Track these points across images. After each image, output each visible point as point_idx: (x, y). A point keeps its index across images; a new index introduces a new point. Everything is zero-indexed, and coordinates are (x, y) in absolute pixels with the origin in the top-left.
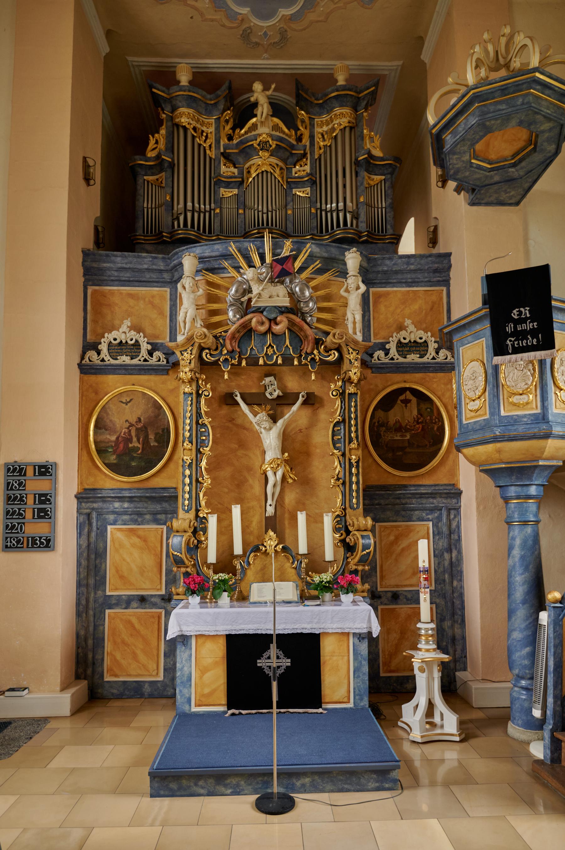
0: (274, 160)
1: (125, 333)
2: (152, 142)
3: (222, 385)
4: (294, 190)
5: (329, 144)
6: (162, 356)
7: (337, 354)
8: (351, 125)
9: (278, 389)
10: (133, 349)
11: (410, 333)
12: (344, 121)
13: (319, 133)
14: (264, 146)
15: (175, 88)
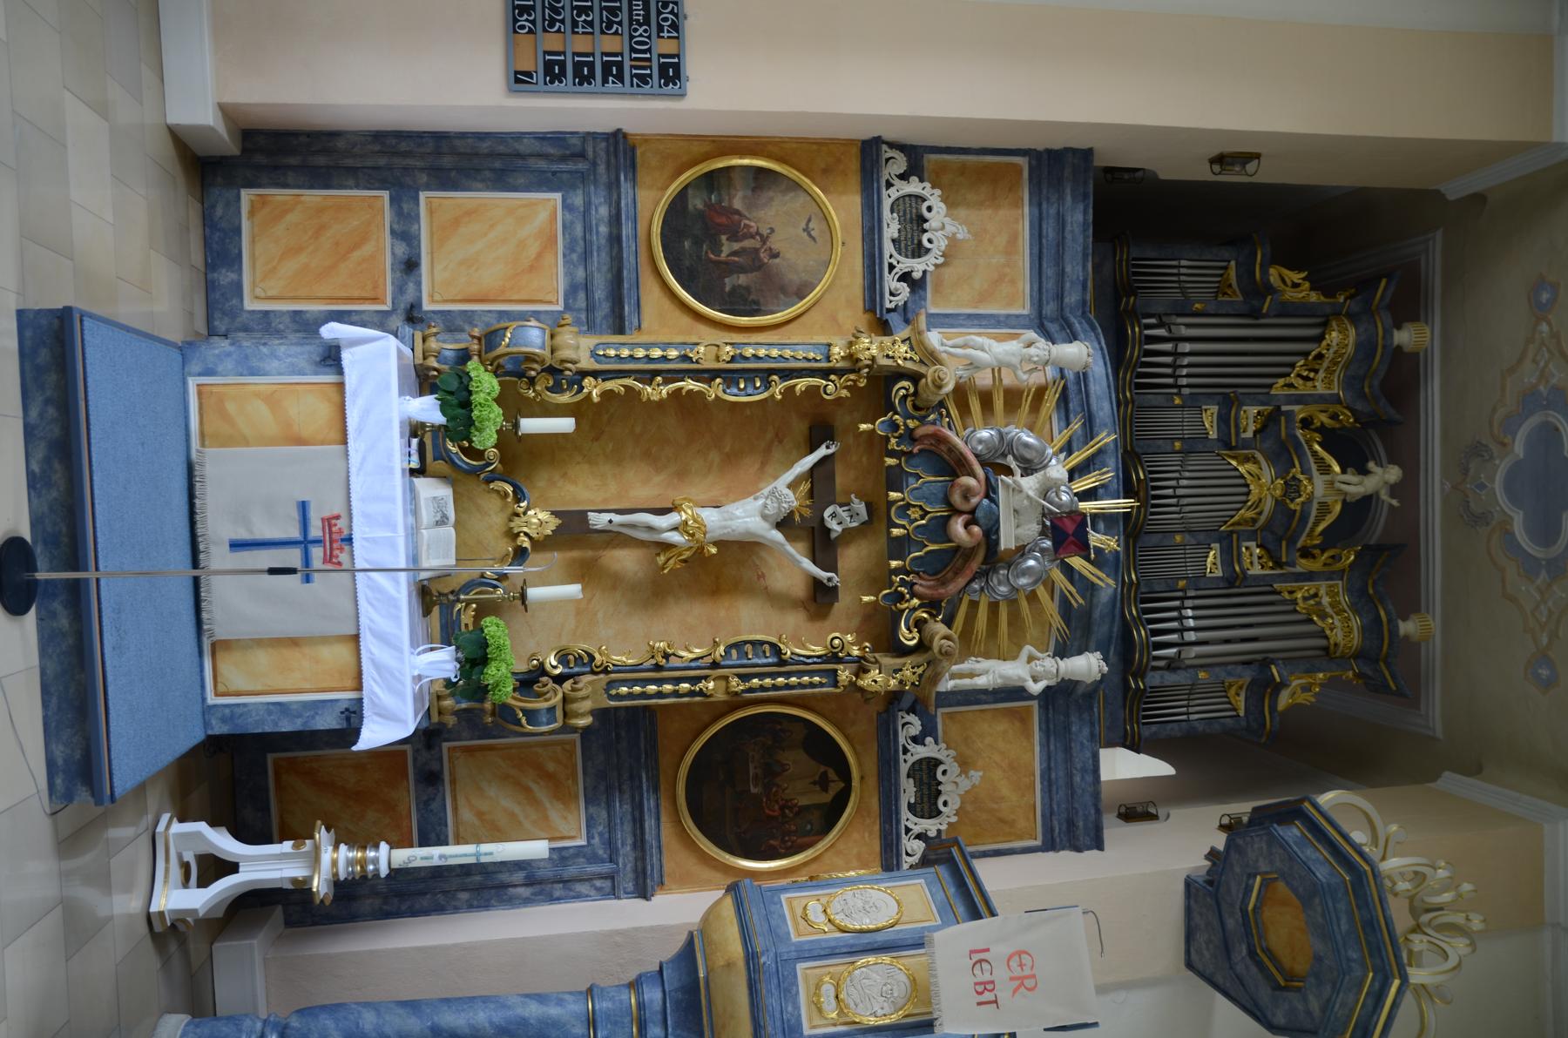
0: (1268, 506)
1: (943, 228)
2: (1296, 277)
4: (1216, 546)
5: (1298, 609)
6: (900, 300)
8: (1332, 647)
9: (843, 530)
10: (913, 243)
12: (1337, 636)
13: (1318, 589)
14: (1292, 488)
15: (1389, 321)
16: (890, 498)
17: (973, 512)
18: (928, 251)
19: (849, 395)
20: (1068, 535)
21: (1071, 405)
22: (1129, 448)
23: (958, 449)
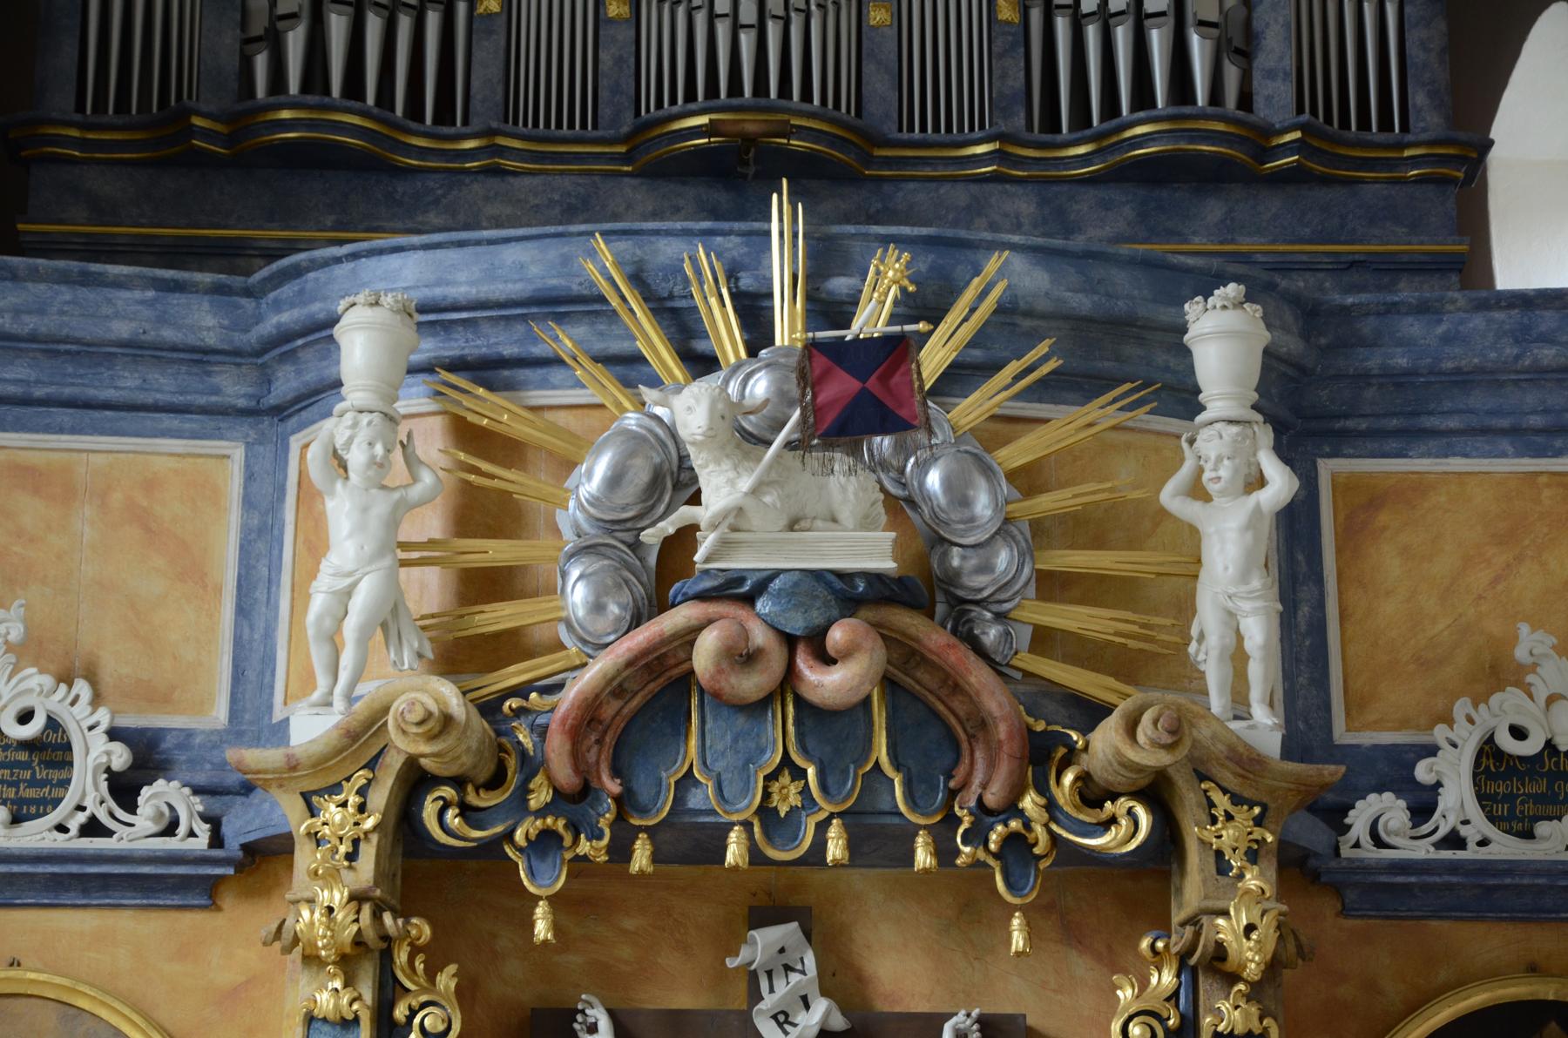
3: (514, 968)
6: (188, 807)
7: (1144, 819)
9: (825, 993)
10: (26, 765)
11: (1551, 700)
16: (743, 863)
17: (790, 641)
18: (52, 723)
19: (452, 968)
20: (864, 392)
21: (509, 351)
22: (622, 149)
23: (619, 672)
